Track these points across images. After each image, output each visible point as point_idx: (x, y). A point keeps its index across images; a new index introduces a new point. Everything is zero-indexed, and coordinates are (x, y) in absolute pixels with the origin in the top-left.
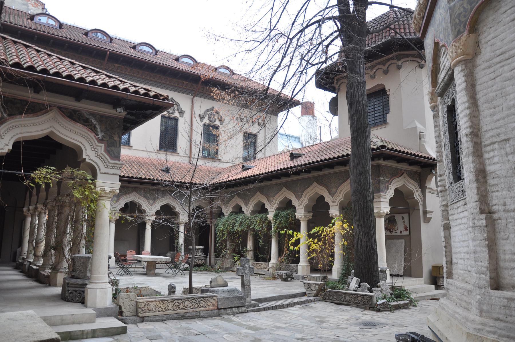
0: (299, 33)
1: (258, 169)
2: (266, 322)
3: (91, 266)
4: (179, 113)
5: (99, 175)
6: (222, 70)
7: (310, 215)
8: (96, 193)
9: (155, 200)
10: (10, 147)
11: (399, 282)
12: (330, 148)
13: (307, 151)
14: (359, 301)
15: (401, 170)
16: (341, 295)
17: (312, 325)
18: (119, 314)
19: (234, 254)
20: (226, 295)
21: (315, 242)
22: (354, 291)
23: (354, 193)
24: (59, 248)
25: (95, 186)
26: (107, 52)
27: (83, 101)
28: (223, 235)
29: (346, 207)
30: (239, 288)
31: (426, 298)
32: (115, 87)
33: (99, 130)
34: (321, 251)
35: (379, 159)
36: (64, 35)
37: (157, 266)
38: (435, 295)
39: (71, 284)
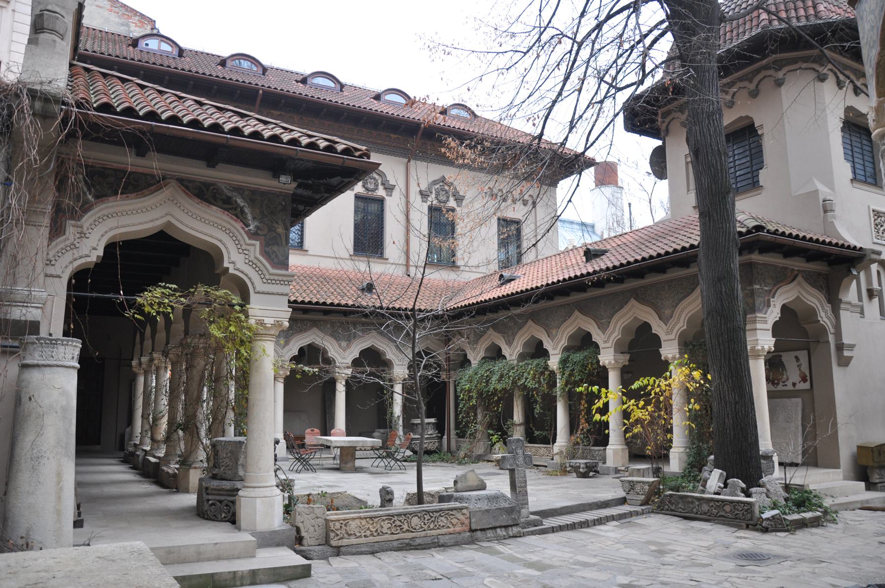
1: (528, 279)
2: (559, 554)
3: (245, 457)
4: (385, 188)
5: (253, 296)
6: (454, 112)
7: (624, 359)
8: (249, 329)
9: (350, 341)
10: (101, 254)
11: (798, 477)
12: (656, 237)
13: (614, 245)
15: (793, 270)
16: (692, 503)
17: (645, 558)
18: (297, 541)
19: (491, 432)
20: (484, 506)
21: (640, 406)
22: (715, 494)
23: (709, 314)
24: (190, 426)
25: (247, 317)
26: (258, 91)
27: (220, 166)
28: (470, 398)
29: (691, 343)
30: (507, 490)
31: (851, 507)
32: (275, 138)
33: (249, 217)
34: (651, 423)
35: (751, 252)
36: (187, 67)
37: (358, 454)
38: (867, 501)
39: (212, 489)
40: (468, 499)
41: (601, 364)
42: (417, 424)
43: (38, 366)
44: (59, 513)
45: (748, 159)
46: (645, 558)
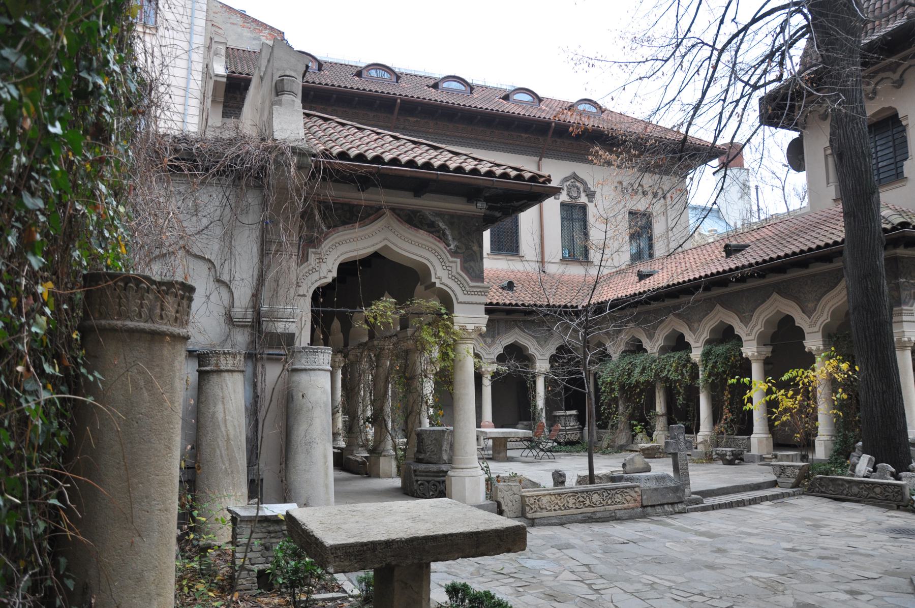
0: (763, 61)
2: (724, 526)
7: (767, 351)
12: (796, 232)
13: (754, 240)
14: (876, 494)
16: (842, 485)
17: (803, 530)
19: (635, 423)
20: (653, 485)
21: (789, 396)
23: (855, 309)
24: (377, 419)
25: (453, 324)
26: (396, 100)
28: (612, 390)
29: (835, 335)
33: (450, 238)
34: (800, 411)
37: (509, 445)
40: (638, 479)
41: (744, 356)
42: (559, 416)
43: (305, 370)
44: (327, 486)
45: (891, 149)
46: (803, 530)
